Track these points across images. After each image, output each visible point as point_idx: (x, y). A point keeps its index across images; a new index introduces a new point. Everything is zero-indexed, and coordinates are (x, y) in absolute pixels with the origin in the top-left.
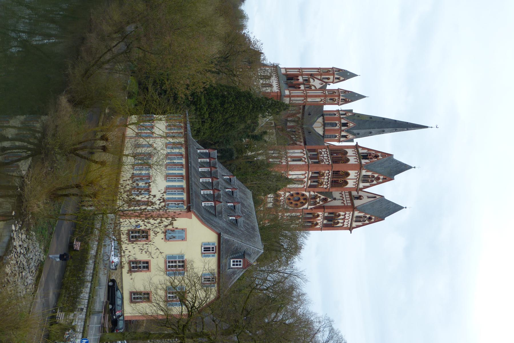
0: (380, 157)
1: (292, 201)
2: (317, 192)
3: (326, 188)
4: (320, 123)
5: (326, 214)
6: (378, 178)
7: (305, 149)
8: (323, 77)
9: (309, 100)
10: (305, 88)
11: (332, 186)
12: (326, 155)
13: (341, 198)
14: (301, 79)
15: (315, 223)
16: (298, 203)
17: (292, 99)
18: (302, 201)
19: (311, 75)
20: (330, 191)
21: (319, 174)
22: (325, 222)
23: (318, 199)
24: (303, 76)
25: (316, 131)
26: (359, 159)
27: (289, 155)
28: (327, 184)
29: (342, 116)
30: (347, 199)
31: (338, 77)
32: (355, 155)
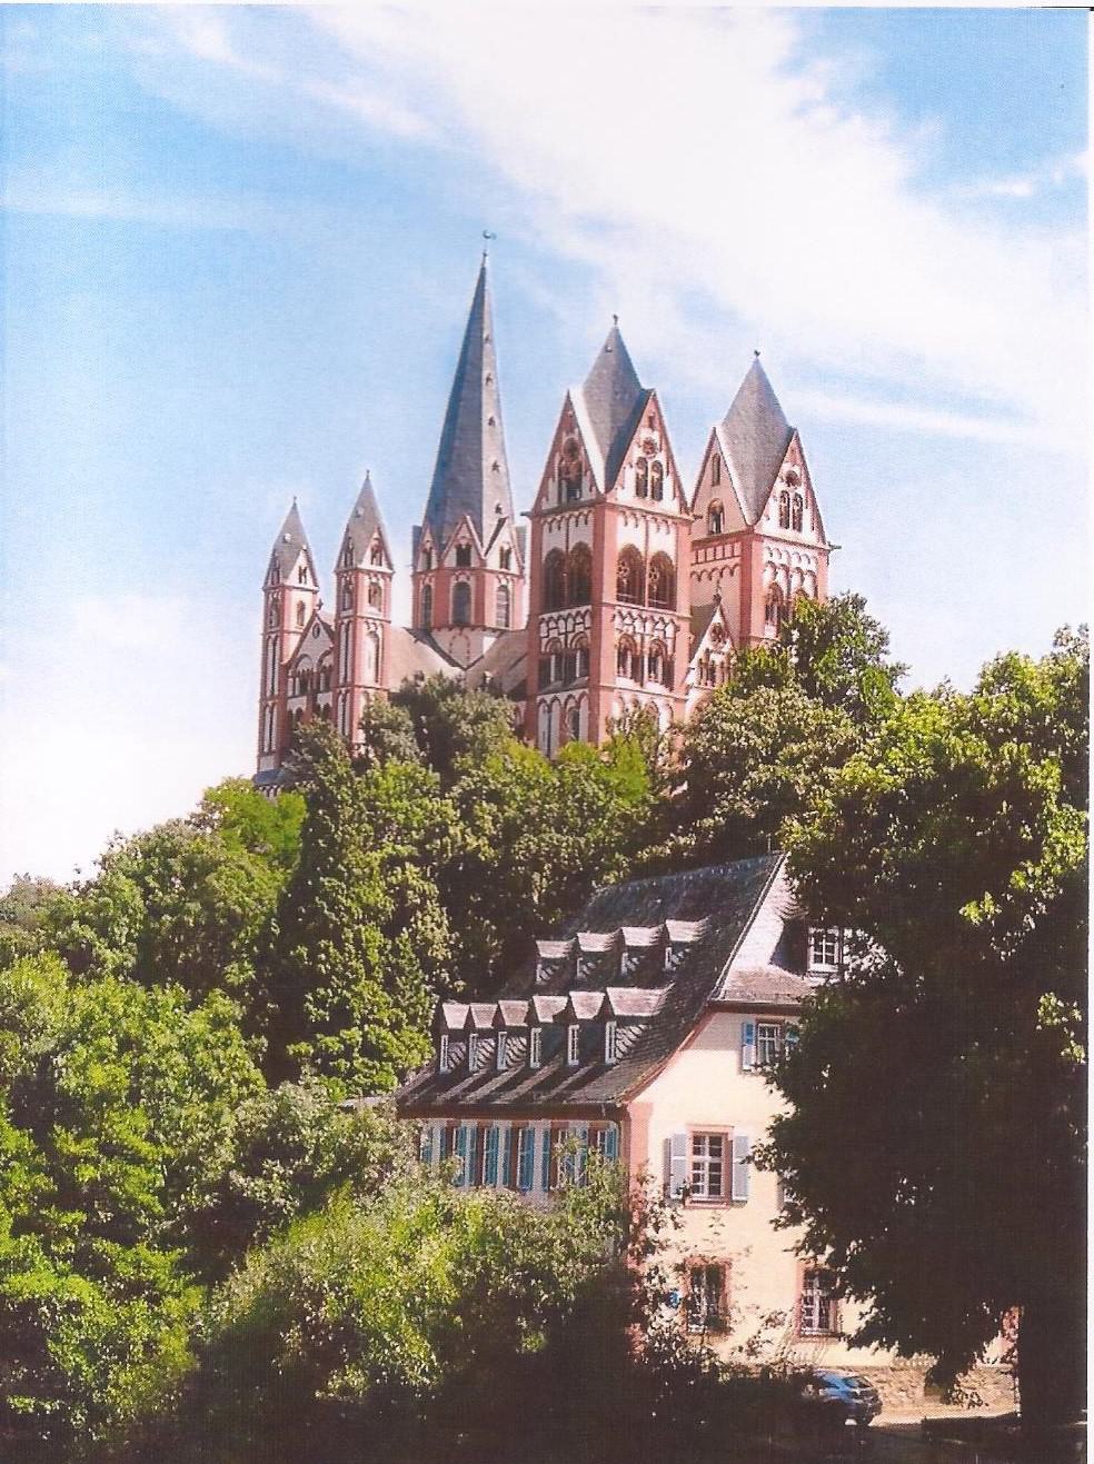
2: (691, 658)
3: (677, 629)
6: (649, 446)
7: (539, 698)
10: (327, 689)
12: (562, 622)
13: (715, 575)
14: (299, 704)
20: (683, 609)
21: (626, 649)
23: (713, 656)
24: (290, 693)
28: (660, 626)
29: (434, 566)
31: (294, 574)
32: (563, 525)
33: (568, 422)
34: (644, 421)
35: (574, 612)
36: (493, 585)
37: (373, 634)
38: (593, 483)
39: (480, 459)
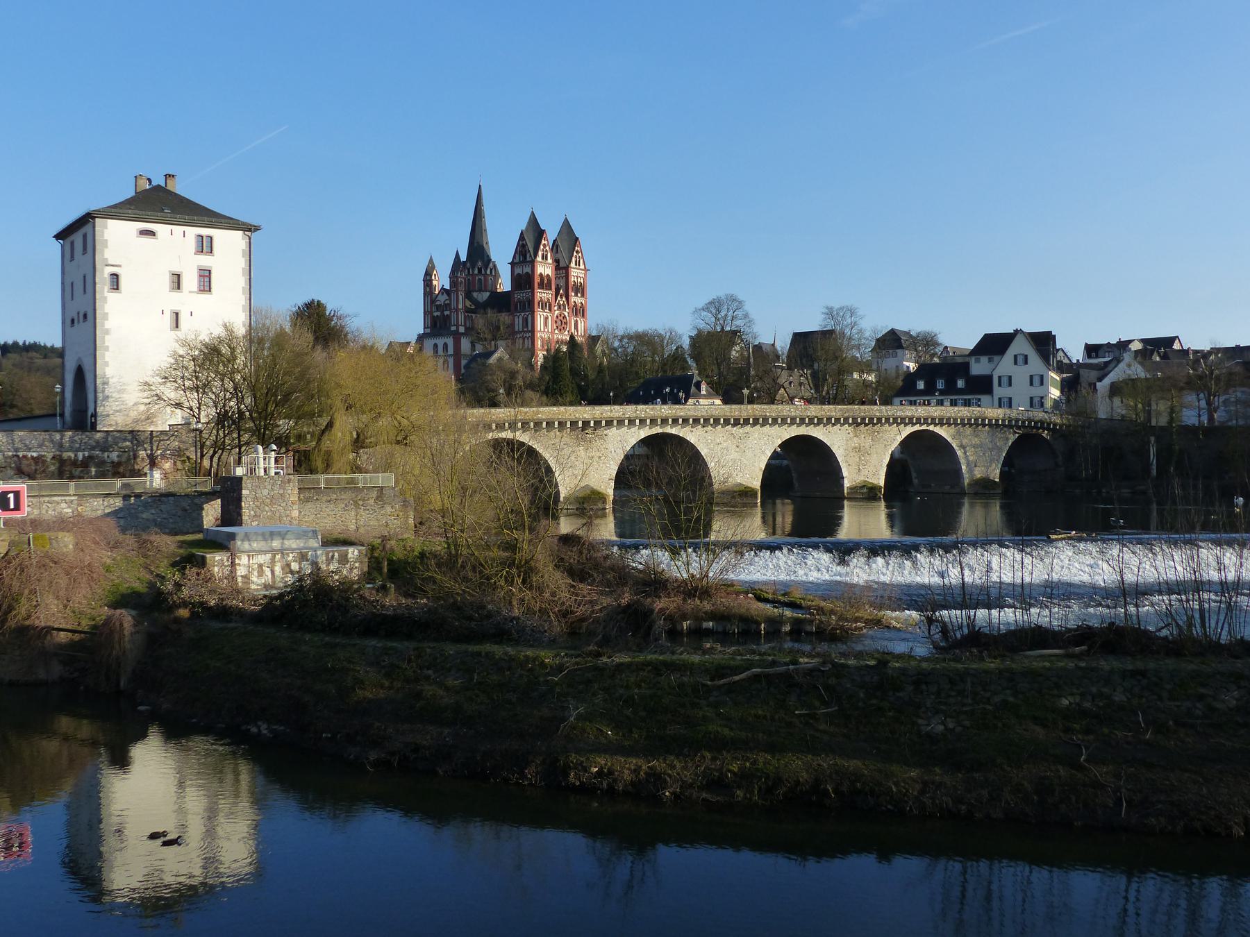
5: (573, 294)
6: (544, 244)
10: (446, 310)
11: (551, 289)
14: (435, 314)
16: (564, 321)
17: (460, 324)
18: (561, 318)
22: (579, 295)
27: (521, 330)
29: (471, 273)
33: (522, 237)
38: (531, 256)
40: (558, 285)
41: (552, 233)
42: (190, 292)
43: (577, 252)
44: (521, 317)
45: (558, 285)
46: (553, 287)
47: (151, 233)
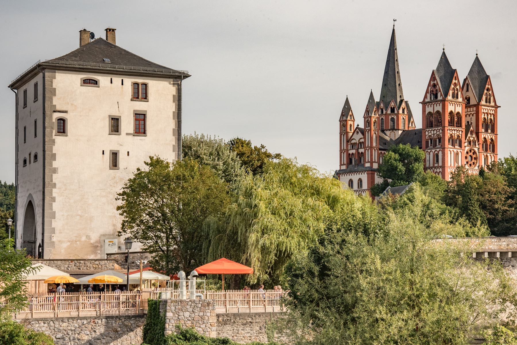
0: (435, 82)
1: (472, 163)
2: (465, 140)
3: (462, 132)
4: (391, 134)
5: (483, 130)
6: (455, 83)
8: (349, 130)
9: (374, 145)
10: (361, 148)
11: (461, 126)
12: (432, 132)
14: (351, 152)
15: (490, 141)
17: (374, 160)
18: (471, 154)
19: (348, 141)
20: (464, 127)
22: (489, 131)
23: (471, 138)
24: (349, 149)
25: (399, 138)
26: (437, 102)
27: (431, 165)
29: (384, 112)
30: (469, 110)
33: (433, 77)
34: (454, 78)
35: (436, 129)
36: (401, 117)
37: (375, 133)
39: (396, 83)
40: (468, 122)
41: (463, 73)
42: (127, 134)
43: (488, 90)
44: (431, 154)
45: (468, 122)
46: (464, 124)
47: (95, 83)
